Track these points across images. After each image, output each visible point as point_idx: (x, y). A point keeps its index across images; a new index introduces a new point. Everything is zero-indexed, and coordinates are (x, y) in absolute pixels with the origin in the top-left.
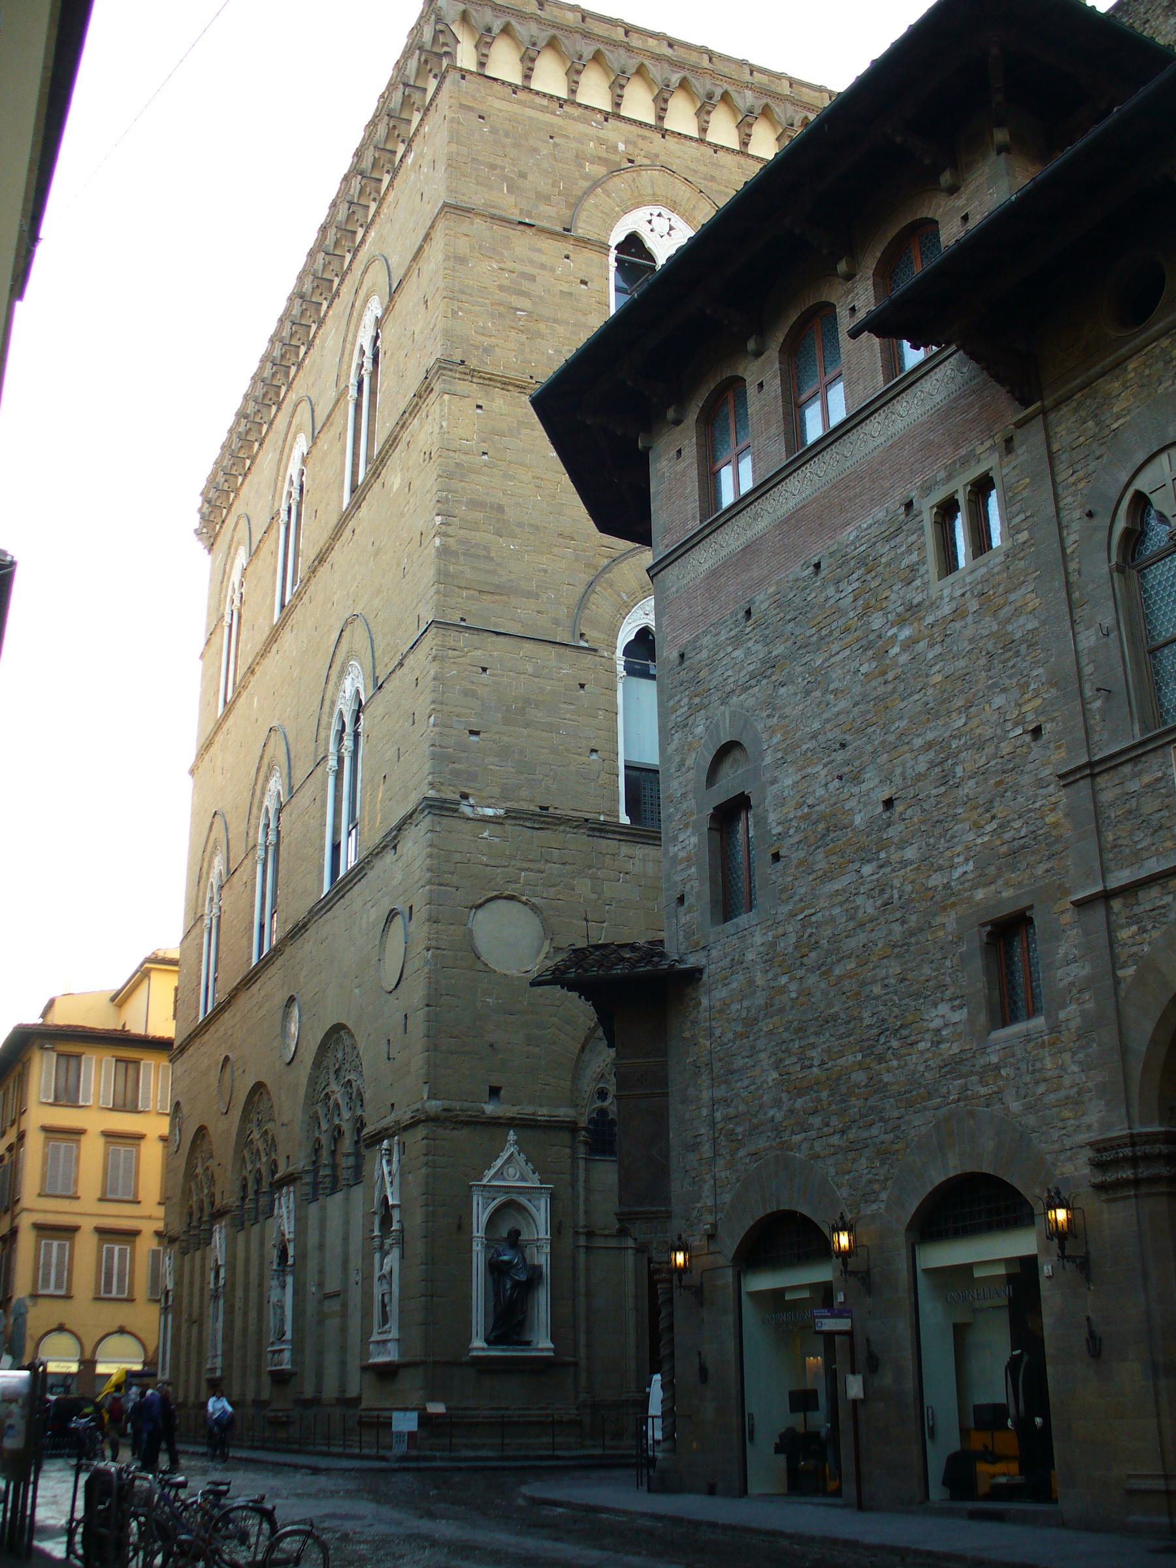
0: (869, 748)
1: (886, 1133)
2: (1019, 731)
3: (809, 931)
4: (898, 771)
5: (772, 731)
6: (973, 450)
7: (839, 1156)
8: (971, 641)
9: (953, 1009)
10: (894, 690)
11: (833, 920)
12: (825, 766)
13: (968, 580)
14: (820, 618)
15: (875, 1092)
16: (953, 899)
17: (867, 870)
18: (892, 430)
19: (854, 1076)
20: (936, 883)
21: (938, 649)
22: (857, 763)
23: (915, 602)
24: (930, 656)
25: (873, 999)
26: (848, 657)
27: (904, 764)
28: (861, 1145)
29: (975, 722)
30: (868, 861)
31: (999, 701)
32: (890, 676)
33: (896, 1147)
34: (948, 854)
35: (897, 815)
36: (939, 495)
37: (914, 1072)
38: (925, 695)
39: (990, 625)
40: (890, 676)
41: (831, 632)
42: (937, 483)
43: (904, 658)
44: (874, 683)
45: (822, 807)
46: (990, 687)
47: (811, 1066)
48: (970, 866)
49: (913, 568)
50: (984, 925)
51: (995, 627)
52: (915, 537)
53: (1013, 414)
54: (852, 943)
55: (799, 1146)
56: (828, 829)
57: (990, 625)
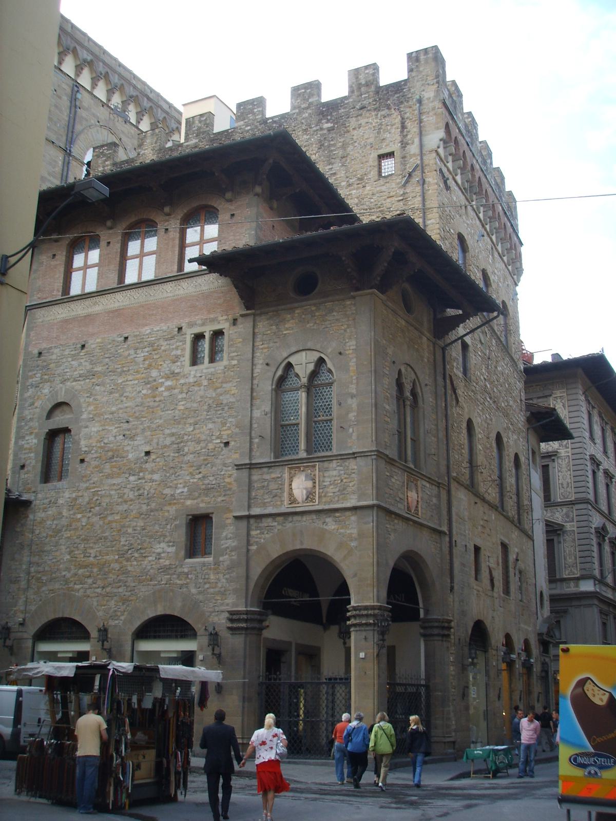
0: (141, 427)
1: (126, 591)
2: (218, 441)
3: (96, 498)
4: (155, 441)
5: (89, 404)
6: (217, 317)
7: (100, 598)
8: (201, 397)
9: (169, 546)
10: (158, 406)
11: (111, 496)
12: (116, 428)
13: (205, 371)
14: (124, 362)
15: (123, 573)
16: (175, 501)
17: (132, 478)
18: (177, 292)
19: (112, 565)
20: (167, 493)
21: (184, 395)
22: (134, 431)
23: (176, 371)
24: (180, 397)
25: (127, 534)
26: (137, 384)
27: (158, 439)
28: (112, 595)
29: (197, 431)
30: (133, 475)
31: (210, 426)
32: (157, 399)
33: (131, 598)
34: (175, 482)
35: (151, 459)
36: (197, 330)
37: (145, 569)
38: (174, 412)
39: (211, 393)
40: (157, 399)
41: (129, 370)
42: (196, 324)
43: (166, 394)
44: (148, 400)
45: (112, 445)
46: (208, 419)
47: (89, 557)
48: (186, 490)
49: (177, 357)
50: (188, 515)
51: (214, 395)
52: (181, 344)
53: (238, 309)
54: (120, 508)
55: (78, 590)
56: (113, 456)
57: (211, 393)
